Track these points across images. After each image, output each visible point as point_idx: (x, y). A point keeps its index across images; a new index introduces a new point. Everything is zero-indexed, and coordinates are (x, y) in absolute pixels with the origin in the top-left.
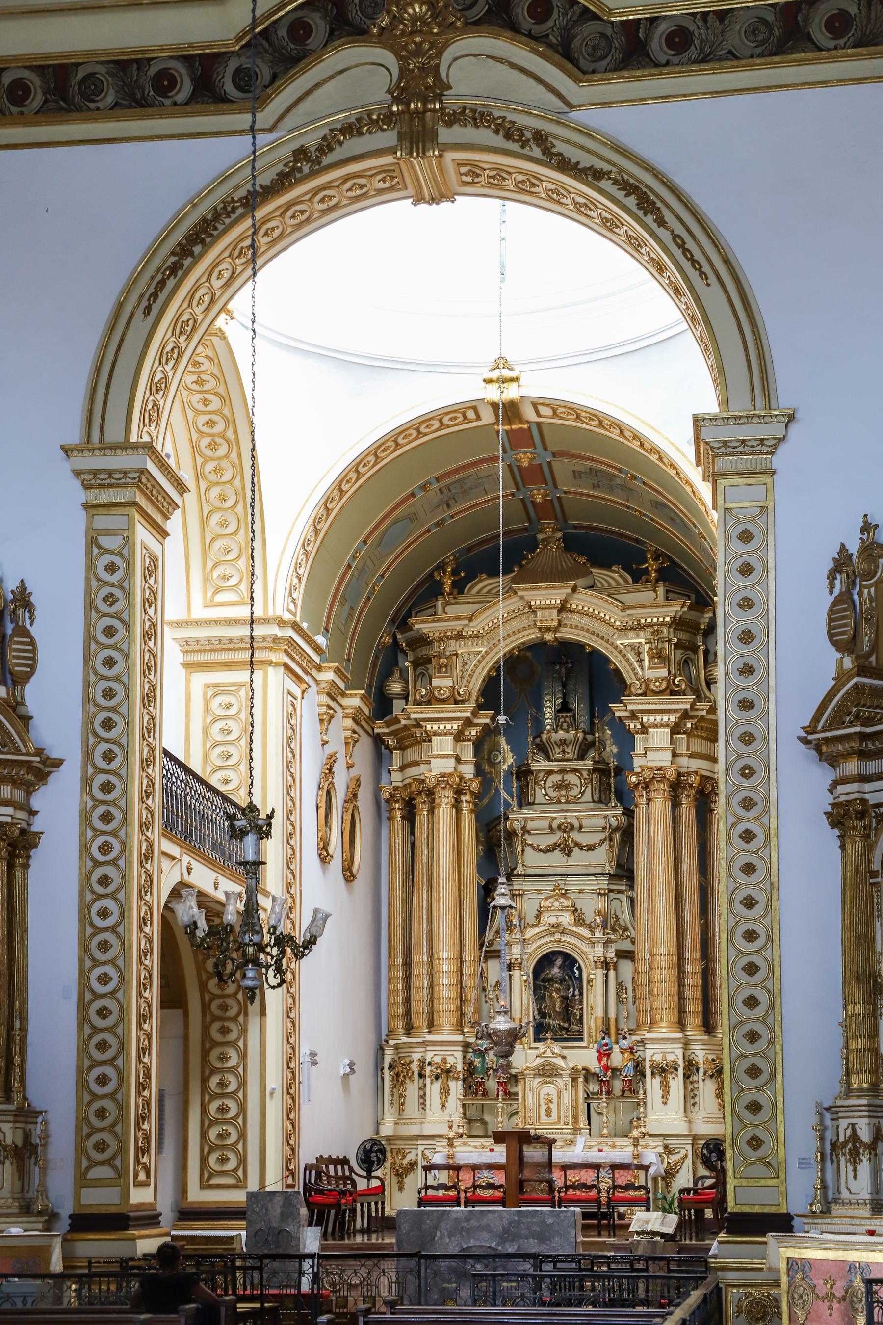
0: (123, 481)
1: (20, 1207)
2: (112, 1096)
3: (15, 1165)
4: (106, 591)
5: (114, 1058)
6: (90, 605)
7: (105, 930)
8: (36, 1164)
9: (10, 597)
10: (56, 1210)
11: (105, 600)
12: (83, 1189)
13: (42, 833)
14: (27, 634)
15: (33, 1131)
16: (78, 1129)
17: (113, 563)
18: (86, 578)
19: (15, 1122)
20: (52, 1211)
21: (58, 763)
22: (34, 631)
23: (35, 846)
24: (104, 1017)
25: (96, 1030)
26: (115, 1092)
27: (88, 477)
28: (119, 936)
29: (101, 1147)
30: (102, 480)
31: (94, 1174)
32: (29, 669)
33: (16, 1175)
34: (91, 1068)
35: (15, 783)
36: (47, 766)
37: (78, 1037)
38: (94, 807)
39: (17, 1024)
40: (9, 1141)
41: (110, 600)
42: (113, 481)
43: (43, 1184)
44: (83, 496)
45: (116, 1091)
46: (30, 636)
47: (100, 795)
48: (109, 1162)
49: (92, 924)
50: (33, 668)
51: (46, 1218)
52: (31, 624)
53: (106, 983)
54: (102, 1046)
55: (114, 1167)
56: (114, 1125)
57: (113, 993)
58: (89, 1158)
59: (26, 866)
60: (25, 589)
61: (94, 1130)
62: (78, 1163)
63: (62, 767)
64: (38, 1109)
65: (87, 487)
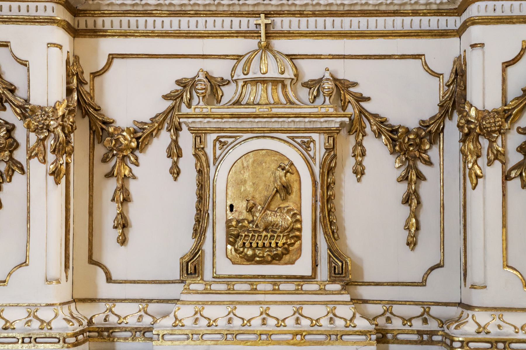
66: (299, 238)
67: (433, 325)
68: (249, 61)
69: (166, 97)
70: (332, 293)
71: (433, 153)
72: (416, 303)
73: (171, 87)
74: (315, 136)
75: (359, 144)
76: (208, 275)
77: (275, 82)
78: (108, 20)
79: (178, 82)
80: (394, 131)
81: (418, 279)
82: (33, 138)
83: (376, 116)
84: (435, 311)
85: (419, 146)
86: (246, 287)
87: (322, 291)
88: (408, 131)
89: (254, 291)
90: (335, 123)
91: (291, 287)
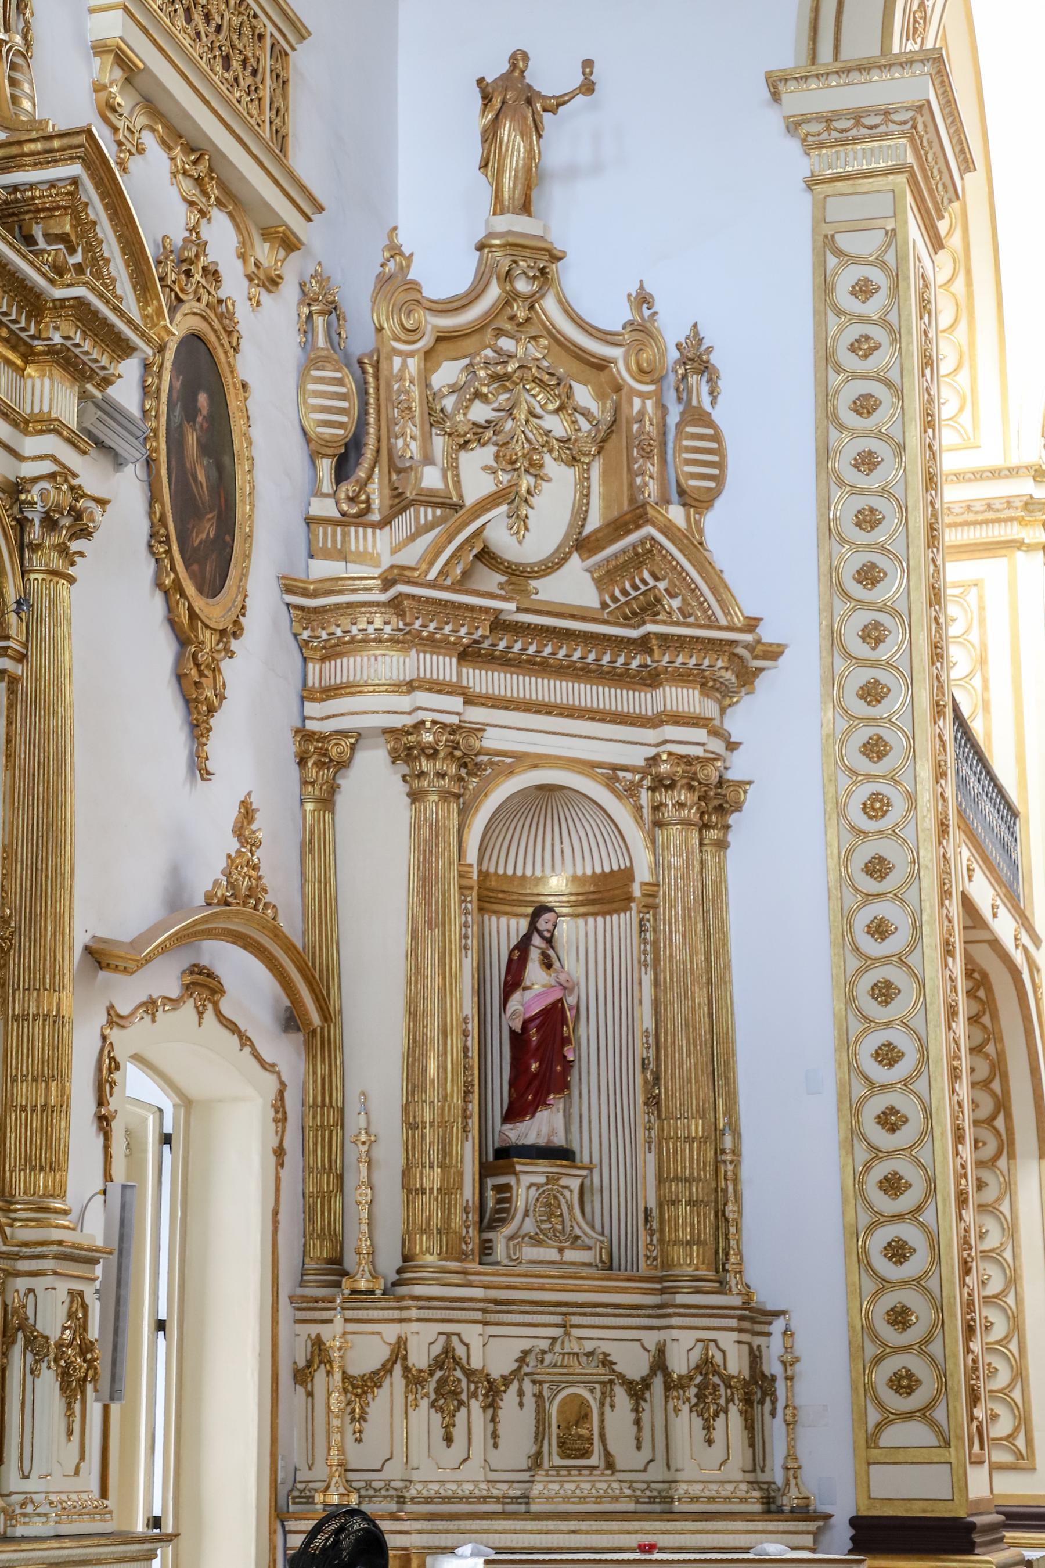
0: (882, 129)
4: (854, 332)
5: (919, 1209)
6: (827, 358)
9: (674, 355)
11: (852, 348)
13: (750, 783)
14: (703, 418)
16: (855, 1351)
17: (867, 280)
18: (816, 312)
19: (741, 1330)
21: (774, 653)
22: (717, 415)
23: (738, 807)
27: (815, 127)
30: (842, 131)
32: (712, 485)
34: (872, 1228)
35: (707, 684)
36: (756, 657)
37: (843, 1169)
39: (728, 1142)
41: (864, 347)
42: (864, 131)
44: (803, 166)
46: (709, 423)
48: (924, 1414)
50: (719, 480)
52: (713, 403)
56: (927, 1341)
57: (905, 1082)
59: (722, 845)
60: (701, 341)
63: (782, 660)
64: (770, 1307)
65: (809, 146)
66: (592, 1444)
67: (655, 1494)
68: (563, 1343)
69: (516, 1361)
70: (607, 1475)
71: (647, 1395)
74: (597, 1386)
75: (612, 1390)
76: (546, 1465)
77: (574, 1354)
79: (522, 1352)
80: (631, 1382)
81: (642, 1468)
82: (472, 1387)
84: (653, 1485)
85: (642, 1391)
87: (602, 1474)
88: (637, 1384)
89: (570, 1475)
91: (587, 1472)
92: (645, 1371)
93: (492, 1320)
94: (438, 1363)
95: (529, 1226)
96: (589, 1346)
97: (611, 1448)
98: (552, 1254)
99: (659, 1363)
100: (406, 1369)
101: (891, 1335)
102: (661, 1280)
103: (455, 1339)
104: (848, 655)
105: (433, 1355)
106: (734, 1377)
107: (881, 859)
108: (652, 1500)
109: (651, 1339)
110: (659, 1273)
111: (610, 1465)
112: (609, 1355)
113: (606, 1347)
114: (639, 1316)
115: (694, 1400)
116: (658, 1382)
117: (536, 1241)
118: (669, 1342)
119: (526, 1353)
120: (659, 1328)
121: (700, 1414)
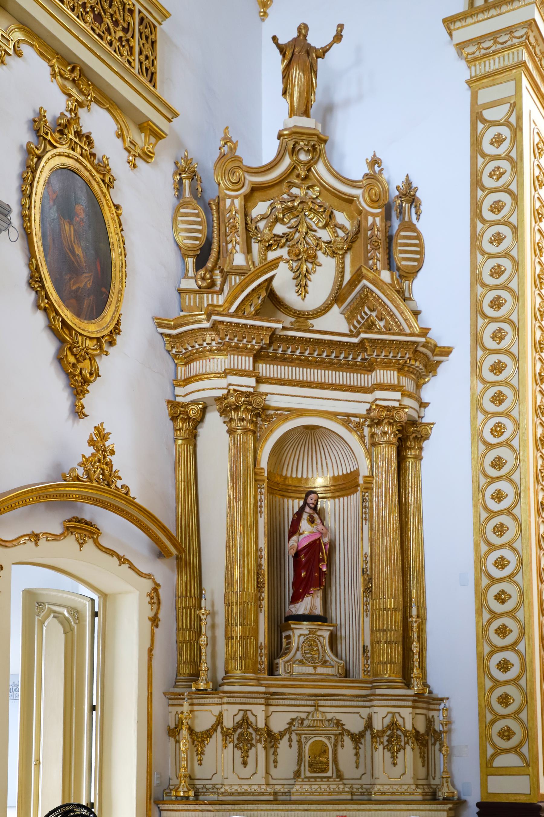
1: (425, 794)
2: (515, 681)
3: (417, 751)
5: (515, 643)
7: (500, 513)
8: (440, 751)
10: (463, 797)
12: (489, 777)
15: (436, 717)
16: (482, 717)
20: (459, 799)
24: (503, 602)
25: (495, 616)
26: (519, 677)
28: (515, 518)
29: (506, 734)
31: (501, 761)
33: (420, 761)
34: (491, 653)
38: (485, 390)
40: (409, 727)
43: (448, 771)
45: (518, 676)
47: (490, 377)
49: (486, 508)
51: (451, 806)
53: (503, 567)
54: (503, 631)
55: (521, 755)
56: (518, 712)
57: (511, 576)
58: (494, 746)
61: (498, 717)
62: (483, 751)
66: (328, 765)
67: (364, 790)
68: (313, 714)
70: (337, 781)
71: (363, 741)
72: (359, 784)
73: (289, 721)
74: (332, 736)
75: (342, 738)
76: (302, 776)
77: (320, 720)
78: (271, 701)
79: (291, 719)
80: (352, 734)
81: (359, 778)
82: (258, 737)
83: (347, 730)
84: (364, 786)
85: (359, 739)
86: (313, 780)
87: (334, 781)
88: (356, 735)
89: (316, 781)
90: (338, 732)
91: (326, 780)
92: (361, 728)
93: (274, 703)
94: (239, 725)
95: (299, 656)
96: (329, 716)
97: (341, 767)
98: (311, 670)
99: (369, 725)
100: (222, 728)
101: (500, 709)
102: (372, 682)
103: (249, 713)
104: (484, 349)
105: (236, 721)
106: (408, 731)
107: (499, 458)
108: (362, 794)
109: (364, 712)
110: (371, 679)
111: (340, 776)
112: (341, 721)
113: (339, 716)
114: (357, 701)
115: (386, 743)
116: (368, 735)
117: (301, 662)
118: (373, 714)
119: (293, 720)
120: (369, 707)
121: (389, 750)
